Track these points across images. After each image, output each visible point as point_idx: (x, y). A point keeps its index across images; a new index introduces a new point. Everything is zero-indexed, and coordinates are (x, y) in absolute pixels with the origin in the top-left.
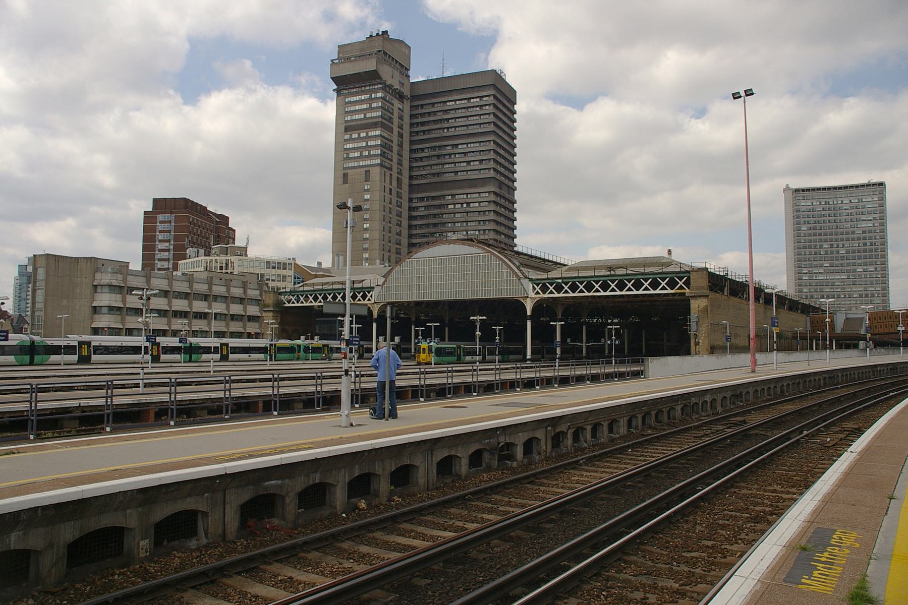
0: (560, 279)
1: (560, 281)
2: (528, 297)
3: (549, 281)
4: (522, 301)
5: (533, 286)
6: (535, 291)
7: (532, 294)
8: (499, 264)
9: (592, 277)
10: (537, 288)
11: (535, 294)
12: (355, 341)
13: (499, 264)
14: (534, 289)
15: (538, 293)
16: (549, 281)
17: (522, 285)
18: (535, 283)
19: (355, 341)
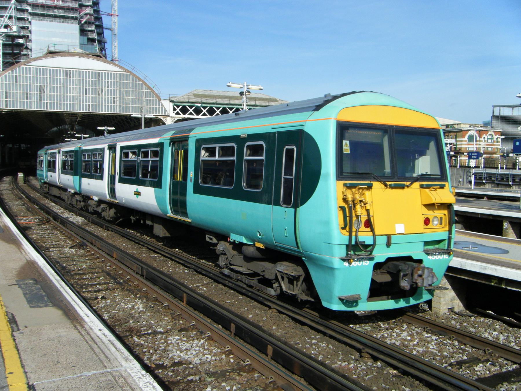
0: (200, 103)
1: (199, 105)
2: (169, 116)
3: (189, 104)
4: (163, 119)
5: (174, 107)
6: (176, 112)
7: (172, 114)
8: (139, 84)
9: (227, 104)
10: (178, 110)
11: (176, 114)
12: (474, 155)
13: (139, 84)
14: (174, 110)
15: (178, 113)
16: (189, 104)
17: (162, 105)
18: (176, 105)
19: (474, 155)
